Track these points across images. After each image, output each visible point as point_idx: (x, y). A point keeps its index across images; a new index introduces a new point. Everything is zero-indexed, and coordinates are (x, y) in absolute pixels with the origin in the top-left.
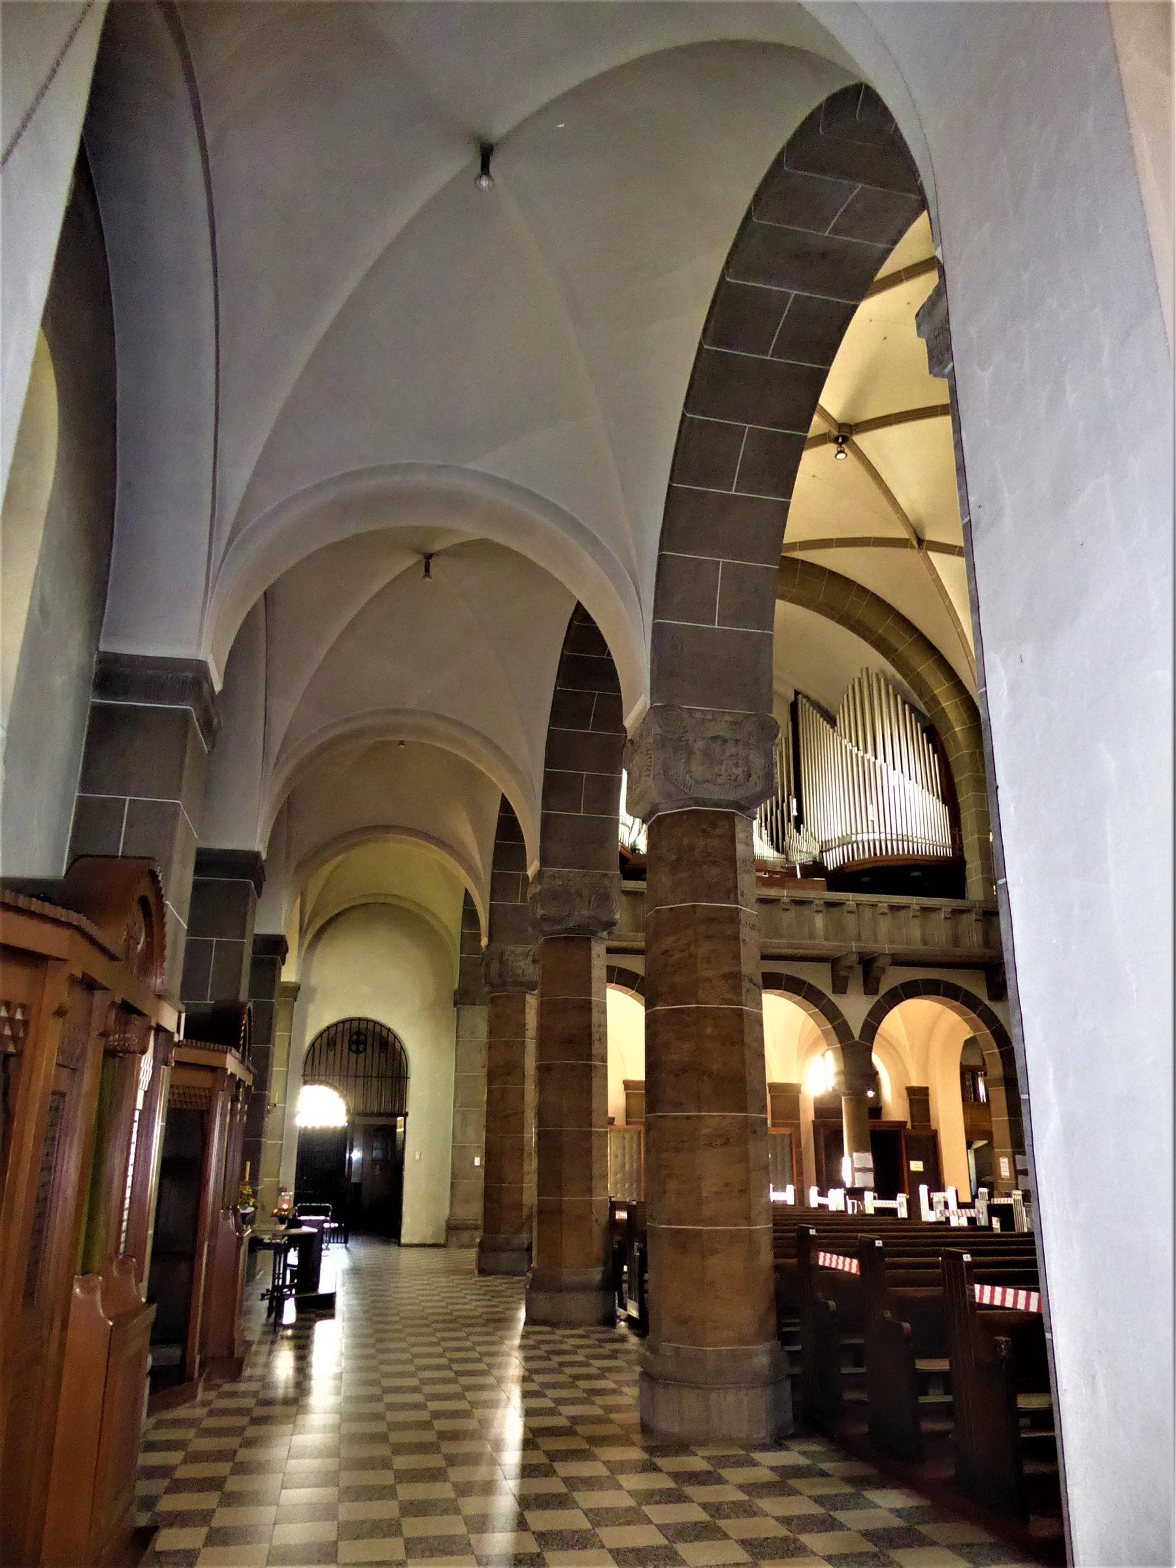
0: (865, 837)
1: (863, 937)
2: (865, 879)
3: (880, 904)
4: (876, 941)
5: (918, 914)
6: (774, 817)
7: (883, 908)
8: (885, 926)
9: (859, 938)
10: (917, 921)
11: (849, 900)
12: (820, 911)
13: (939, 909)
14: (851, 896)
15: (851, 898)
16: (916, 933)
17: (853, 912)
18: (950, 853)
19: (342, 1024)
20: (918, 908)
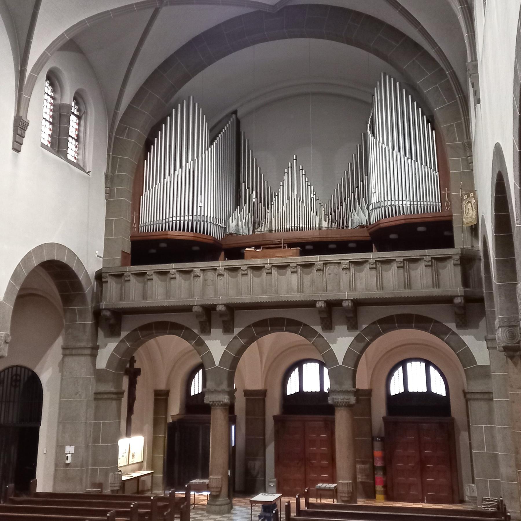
0: (393, 203)
1: (329, 288)
2: (393, 236)
3: (342, 262)
4: (339, 290)
5: (374, 266)
6: (286, 203)
7: (345, 263)
8: (345, 277)
9: (325, 290)
10: (374, 272)
11: (318, 261)
12: (296, 272)
13: (395, 260)
14: (319, 257)
15: (318, 259)
16: (373, 281)
17: (320, 270)
18: (439, 208)
19: (3, 372)
20: (373, 261)
